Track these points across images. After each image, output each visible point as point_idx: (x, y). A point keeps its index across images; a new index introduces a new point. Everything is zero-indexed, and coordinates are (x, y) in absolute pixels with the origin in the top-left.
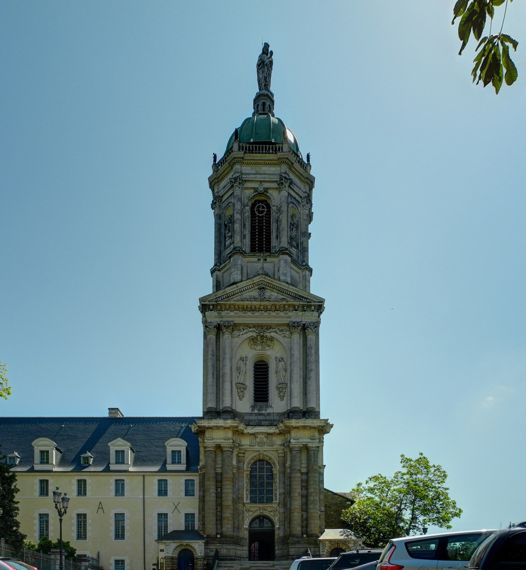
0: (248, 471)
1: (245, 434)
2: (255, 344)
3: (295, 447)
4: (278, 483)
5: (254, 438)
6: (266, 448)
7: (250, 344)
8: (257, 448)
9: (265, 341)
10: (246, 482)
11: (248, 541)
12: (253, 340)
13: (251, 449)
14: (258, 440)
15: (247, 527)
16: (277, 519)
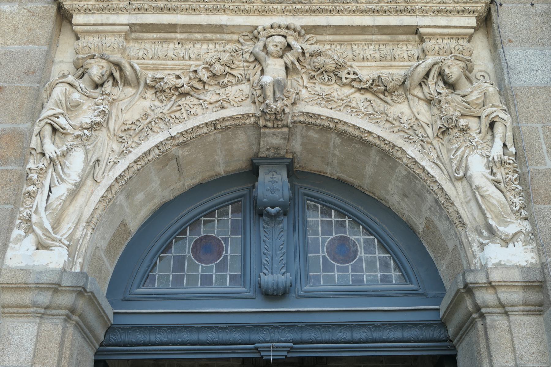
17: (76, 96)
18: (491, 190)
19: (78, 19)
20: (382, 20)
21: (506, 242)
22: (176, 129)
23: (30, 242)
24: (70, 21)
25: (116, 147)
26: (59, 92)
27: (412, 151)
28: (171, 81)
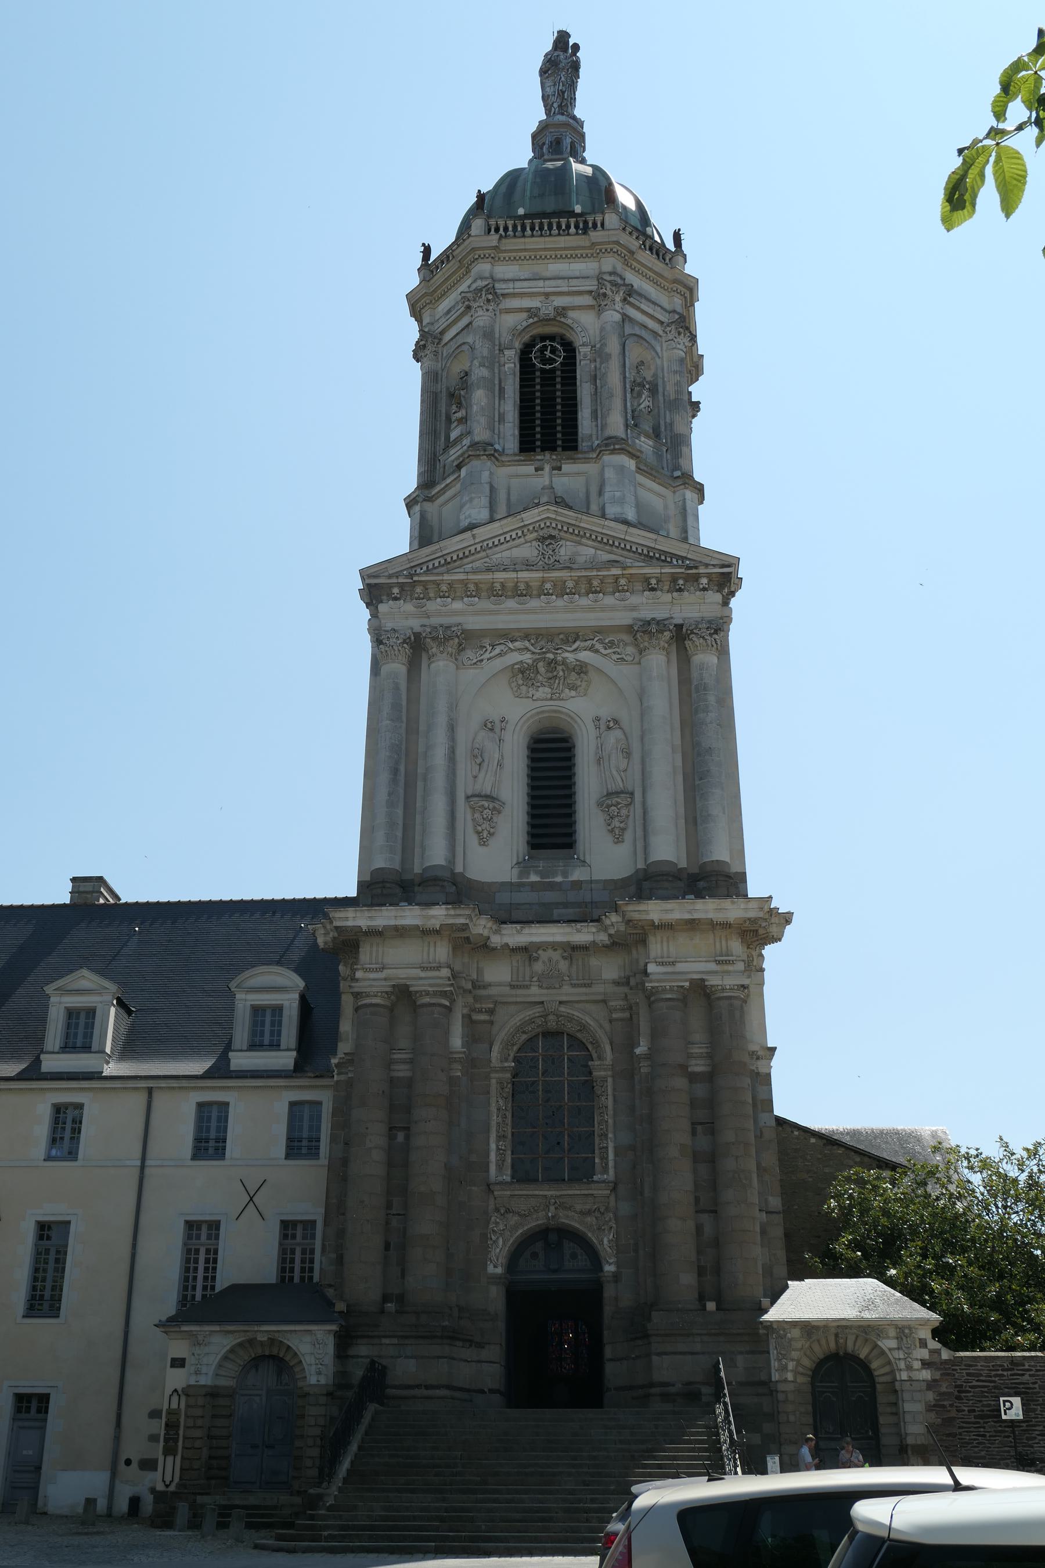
0: (503, 1069)
1: (494, 949)
2: (530, 683)
3: (664, 990)
4: (611, 1112)
5: (527, 963)
6: (567, 992)
7: (515, 684)
8: (535, 992)
9: (561, 673)
10: (498, 1109)
11: (501, 1325)
12: (522, 672)
13: (516, 996)
14: (538, 967)
15: (499, 1270)
16: (609, 1241)
17: (498, 1220)
18: (608, 1249)
19: (496, 1193)
20: (583, 1192)
21: (610, 1264)
22: (526, 1228)
23: (491, 1266)
24: (493, 1192)
25: (509, 1233)
26: (493, 1219)
27: (590, 1235)
28: (523, 1212)
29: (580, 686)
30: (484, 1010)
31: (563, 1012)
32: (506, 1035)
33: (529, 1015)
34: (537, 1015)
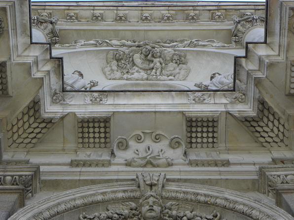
1: (50, 121)
7: (109, 69)
9: (158, 64)
12: (118, 60)
29: (179, 73)
30: (9, 178)
31: (174, 191)
32: (48, 209)
33: (103, 194)
34: (120, 195)
